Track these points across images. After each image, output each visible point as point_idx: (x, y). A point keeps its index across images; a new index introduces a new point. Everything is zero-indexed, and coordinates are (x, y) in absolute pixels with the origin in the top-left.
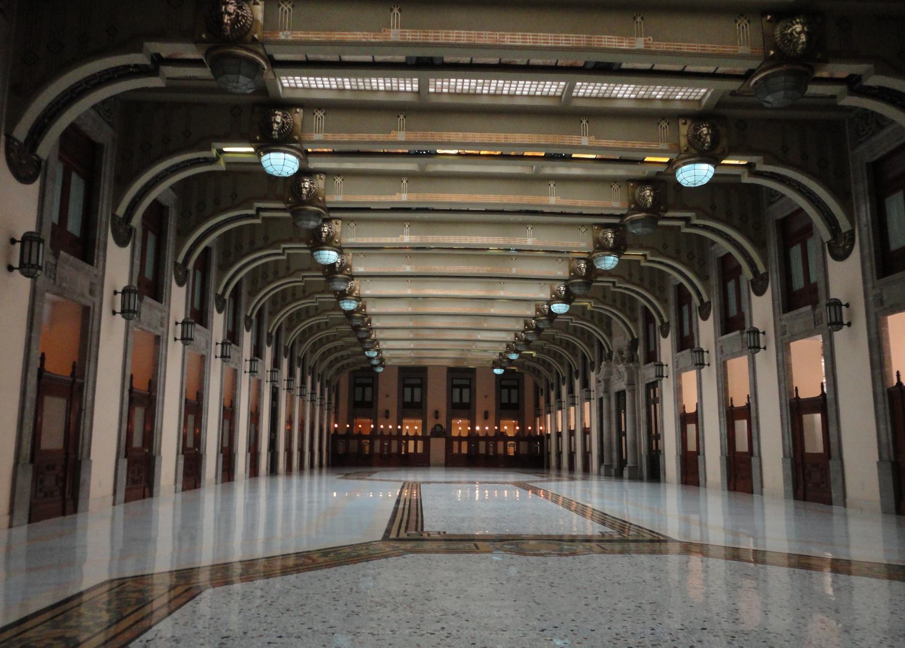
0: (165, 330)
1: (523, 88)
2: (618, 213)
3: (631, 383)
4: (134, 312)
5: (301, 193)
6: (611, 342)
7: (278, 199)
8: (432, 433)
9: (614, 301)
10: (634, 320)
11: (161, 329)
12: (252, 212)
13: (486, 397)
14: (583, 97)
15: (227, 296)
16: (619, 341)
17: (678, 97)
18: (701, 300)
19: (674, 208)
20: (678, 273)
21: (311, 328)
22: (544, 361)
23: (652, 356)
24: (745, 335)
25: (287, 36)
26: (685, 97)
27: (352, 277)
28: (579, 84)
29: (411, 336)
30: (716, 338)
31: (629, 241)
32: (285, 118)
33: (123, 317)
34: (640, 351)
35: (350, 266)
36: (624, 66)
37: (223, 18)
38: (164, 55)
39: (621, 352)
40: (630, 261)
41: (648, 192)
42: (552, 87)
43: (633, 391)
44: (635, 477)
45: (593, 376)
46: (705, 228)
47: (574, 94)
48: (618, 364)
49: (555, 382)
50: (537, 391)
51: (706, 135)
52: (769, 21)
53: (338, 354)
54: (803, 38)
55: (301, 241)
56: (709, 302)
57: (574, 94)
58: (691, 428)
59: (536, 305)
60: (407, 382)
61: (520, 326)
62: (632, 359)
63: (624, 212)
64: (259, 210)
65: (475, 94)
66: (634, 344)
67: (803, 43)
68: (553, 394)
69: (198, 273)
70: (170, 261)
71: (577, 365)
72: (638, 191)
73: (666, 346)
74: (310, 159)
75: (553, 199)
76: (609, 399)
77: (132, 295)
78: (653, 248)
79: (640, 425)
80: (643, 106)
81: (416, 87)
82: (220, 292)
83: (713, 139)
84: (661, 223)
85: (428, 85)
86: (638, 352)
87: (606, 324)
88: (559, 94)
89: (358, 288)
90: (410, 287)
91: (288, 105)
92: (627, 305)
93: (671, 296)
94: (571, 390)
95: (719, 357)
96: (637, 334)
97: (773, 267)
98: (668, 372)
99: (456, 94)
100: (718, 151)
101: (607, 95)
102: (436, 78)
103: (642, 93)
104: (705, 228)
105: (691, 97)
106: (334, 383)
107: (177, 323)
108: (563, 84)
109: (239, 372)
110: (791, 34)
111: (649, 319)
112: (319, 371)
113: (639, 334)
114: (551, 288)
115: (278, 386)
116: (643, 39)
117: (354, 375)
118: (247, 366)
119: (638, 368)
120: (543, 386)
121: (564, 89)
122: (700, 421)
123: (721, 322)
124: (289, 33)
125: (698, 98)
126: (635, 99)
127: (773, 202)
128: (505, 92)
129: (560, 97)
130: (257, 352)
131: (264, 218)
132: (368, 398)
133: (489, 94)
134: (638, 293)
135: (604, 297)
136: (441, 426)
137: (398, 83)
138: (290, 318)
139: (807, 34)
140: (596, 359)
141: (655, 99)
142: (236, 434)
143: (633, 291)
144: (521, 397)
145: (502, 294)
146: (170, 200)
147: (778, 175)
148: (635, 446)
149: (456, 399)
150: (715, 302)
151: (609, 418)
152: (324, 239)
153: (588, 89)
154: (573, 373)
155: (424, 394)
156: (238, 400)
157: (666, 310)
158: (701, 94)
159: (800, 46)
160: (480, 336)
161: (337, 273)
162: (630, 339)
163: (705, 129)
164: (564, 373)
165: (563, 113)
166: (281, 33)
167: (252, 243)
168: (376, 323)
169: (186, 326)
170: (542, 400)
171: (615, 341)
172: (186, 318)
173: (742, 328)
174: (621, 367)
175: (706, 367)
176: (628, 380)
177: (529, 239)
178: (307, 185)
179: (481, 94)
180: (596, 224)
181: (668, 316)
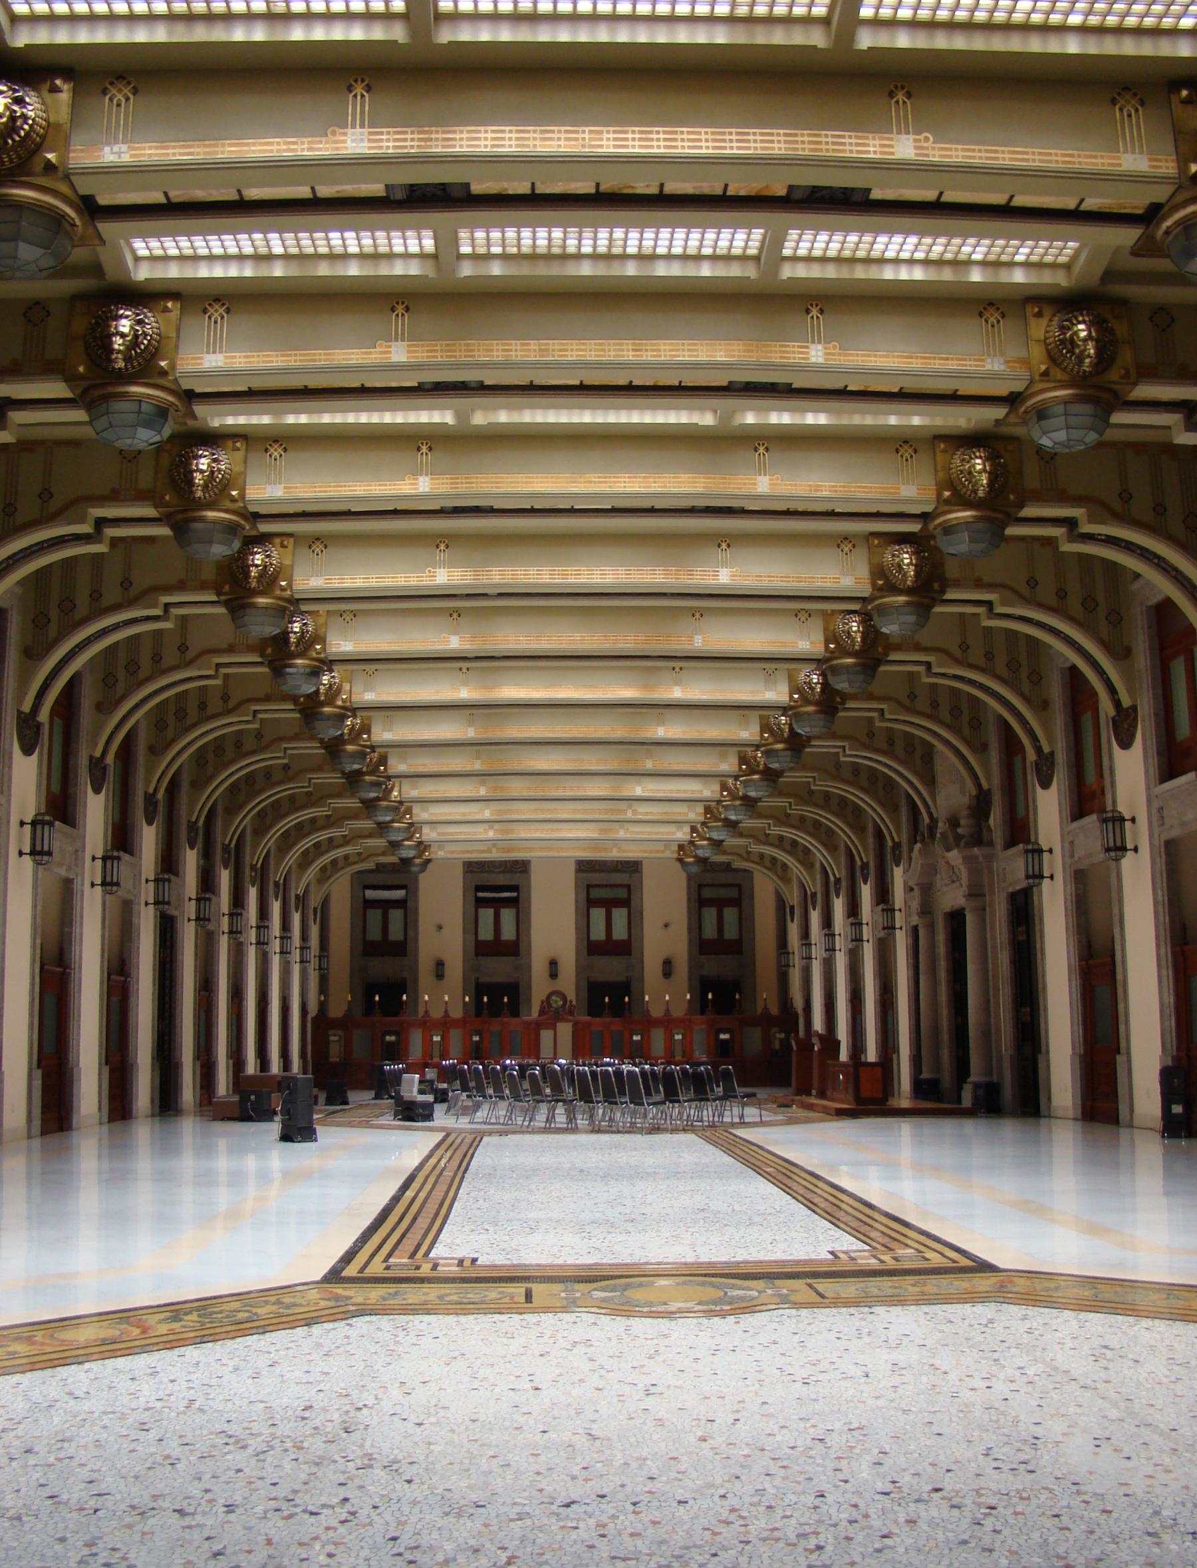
2: (917, 510)
3: (976, 893)
5: (190, 482)
7: (142, 496)
8: (542, 1012)
9: (935, 705)
10: (981, 749)
12: (86, 528)
13: (666, 926)
14: (809, 259)
15: (44, 716)
16: (951, 797)
17: (1020, 258)
18: (1117, 704)
19: (1039, 497)
20: (1067, 643)
21: (250, 779)
23: (1020, 831)
25: (120, 153)
27: (328, 664)
28: (793, 234)
29: (483, 792)
30: (1148, 789)
31: (952, 570)
32: (140, 322)
34: (996, 819)
35: (322, 640)
36: (876, 194)
39: (954, 822)
40: (962, 615)
42: (739, 239)
44: (989, 1105)
45: (898, 877)
46: (1111, 541)
47: (787, 252)
48: (948, 850)
49: (819, 888)
50: (783, 910)
51: (1085, 340)
53: (322, 836)
55: (203, 586)
56: (1134, 708)
57: (787, 252)
61: (728, 765)
62: (979, 838)
63: (929, 508)
64: (101, 523)
65: (564, 257)
68: (815, 917)
71: (865, 854)
73: (1048, 807)
74: (200, 409)
75: (763, 483)
76: (931, 927)
78: (1003, 586)
79: (997, 989)
80: (947, 275)
81: (429, 244)
82: (27, 707)
83: (1100, 350)
84: (1011, 531)
87: (922, 758)
88: (752, 252)
89: (346, 687)
91: (143, 297)
92: (964, 715)
93: (1056, 691)
94: (853, 909)
95: (1156, 831)
96: (988, 778)
98: (1051, 866)
99: (520, 257)
100: (1114, 375)
101: (861, 254)
102: (472, 227)
103: (937, 249)
104: (1111, 541)
105: (1049, 259)
106: (314, 901)
108: (757, 234)
109: (77, 886)
111: (1011, 746)
113: (993, 780)
114: (791, 679)
116: (911, 137)
117: (363, 882)
118: (92, 871)
119: (990, 858)
120: (794, 898)
121: (763, 242)
122: (1119, 977)
123: (1159, 753)
124: (124, 148)
125: (1062, 259)
128: (632, 250)
129: (757, 259)
130: (122, 839)
131: (115, 542)
134: (982, 687)
135: (912, 696)
136: (564, 998)
137: (389, 239)
138: (200, 758)
141: (969, 263)
142: (72, 1024)
144: (746, 922)
145: (677, 693)
148: (987, 1034)
149: (598, 933)
150: (1146, 708)
153: (815, 246)
155: (522, 923)
156: (75, 949)
157: (1047, 725)
161: (294, 656)
162: (974, 792)
163: (1081, 327)
164: (838, 870)
165: (765, 300)
166: (107, 149)
167: (95, 595)
168: (397, 765)
170: (793, 929)
171: (941, 799)
174: (955, 857)
176: (969, 887)
178: (204, 464)
179: (578, 257)
181: (1051, 739)
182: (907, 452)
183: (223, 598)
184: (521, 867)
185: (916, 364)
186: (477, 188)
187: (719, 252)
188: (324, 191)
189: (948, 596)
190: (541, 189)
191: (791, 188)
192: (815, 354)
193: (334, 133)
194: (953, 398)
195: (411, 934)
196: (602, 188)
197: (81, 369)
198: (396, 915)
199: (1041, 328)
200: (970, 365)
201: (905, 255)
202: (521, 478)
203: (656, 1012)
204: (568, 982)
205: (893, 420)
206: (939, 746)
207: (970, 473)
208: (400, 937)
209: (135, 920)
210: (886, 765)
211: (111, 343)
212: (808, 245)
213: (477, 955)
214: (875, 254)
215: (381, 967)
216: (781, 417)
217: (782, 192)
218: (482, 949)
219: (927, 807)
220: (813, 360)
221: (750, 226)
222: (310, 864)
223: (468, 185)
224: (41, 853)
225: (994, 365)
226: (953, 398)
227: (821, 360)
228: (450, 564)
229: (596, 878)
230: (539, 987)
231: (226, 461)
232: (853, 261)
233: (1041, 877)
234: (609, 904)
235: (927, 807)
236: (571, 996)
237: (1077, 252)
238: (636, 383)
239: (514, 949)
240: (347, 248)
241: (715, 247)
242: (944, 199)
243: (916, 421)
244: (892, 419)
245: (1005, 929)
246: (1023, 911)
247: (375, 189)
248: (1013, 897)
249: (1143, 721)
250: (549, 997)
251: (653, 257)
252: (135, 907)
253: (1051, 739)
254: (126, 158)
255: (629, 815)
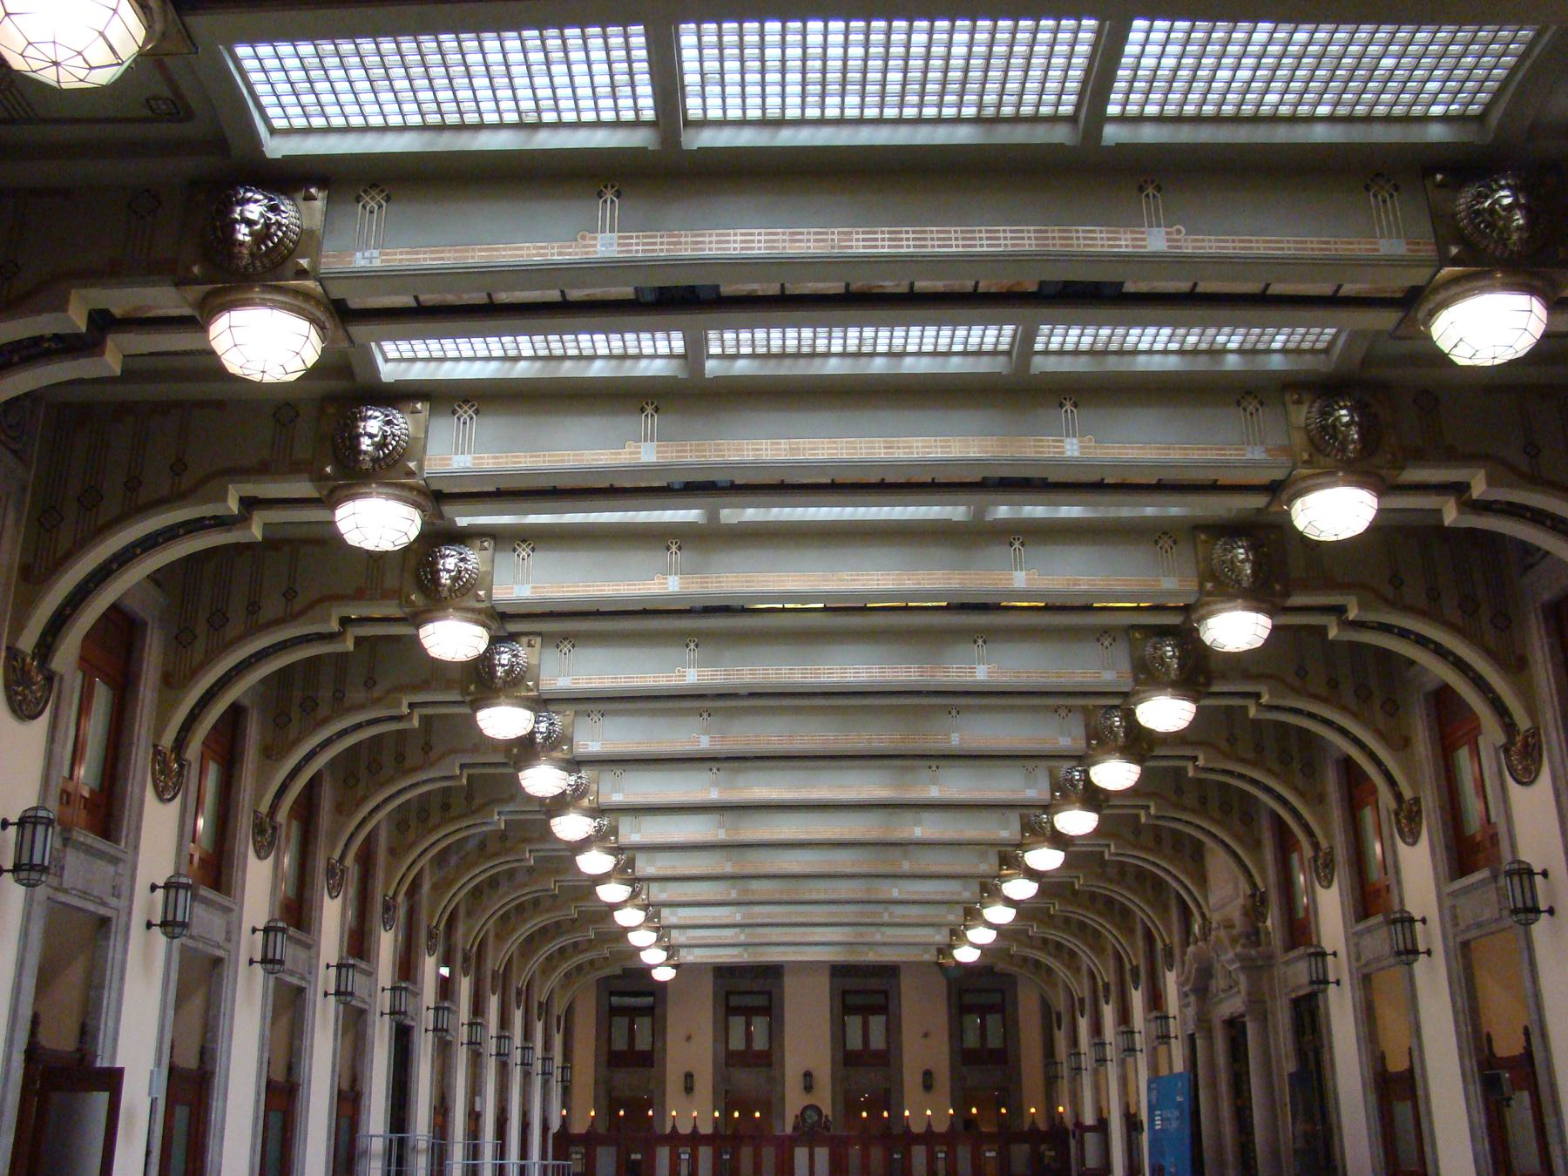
0: (123, 903)
1: (922, 345)
3: (1258, 1004)
4: (44, 869)
5: (436, 580)
6: (1206, 898)
8: (795, 1128)
10: (1255, 845)
11: (113, 902)
14: (1061, 353)
17: (1276, 345)
18: (1398, 797)
19: (1305, 586)
22: (1059, 946)
23: (1300, 931)
24: (1502, 881)
25: (371, 259)
26: (1291, 345)
28: (1045, 329)
29: (734, 895)
30: (1438, 887)
32: (389, 423)
33: (18, 881)
35: (571, 741)
36: (1129, 287)
37: (234, 231)
38: (117, 311)
41: (1241, 553)
43: (1263, 1019)
45: (1171, 982)
49: (1087, 994)
50: (1050, 1020)
51: (1347, 425)
52: (1441, 185)
53: (565, 940)
54: (1519, 219)
56: (1417, 800)
57: (1038, 347)
58: (1403, 1110)
59: (1022, 816)
60: (734, 1001)
63: (1191, 600)
65: (813, 355)
66: (1256, 906)
67: (1519, 228)
68: (1083, 1024)
69: (213, 770)
70: (143, 742)
71: (1136, 956)
72: (1218, 551)
73: (1330, 908)
74: (448, 510)
75: (1023, 577)
77: (40, 829)
78: (1271, 677)
80: (1202, 364)
81: (678, 345)
85: (707, 340)
86: (1269, 923)
87: (1194, 856)
88: (1003, 347)
89: (594, 787)
90: (715, 784)
95: (1450, 932)
96: (1264, 879)
97: (1549, 716)
99: (769, 356)
101: (1113, 347)
102: (722, 328)
103: (1192, 339)
105: (1306, 345)
106: (558, 1008)
107: (153, 888)
108: (1008, 330)
109: (309, 994)
110: (1491, 210)
112: (519, 981)
113: (1268, 880)
114: (1052, 774)
115: (408, 1022)
116: (1163, 230)
120: (1060, 1003)
121: (1014, 337)
122: (1420, 1093)
123: (1447, 847)
124: (376, 253)
125: (1320, 346)
126: (1181, 352)
127: (1531, 566)
128: (881, 348)
129: (1008, 353)
132: (643, 1043)
133: (844, 355)
136: (818, 1111)
139: (1527, 210)
140: (1176, 939)
141: (1224, 351)
143: (1241, 776)
145: (934, 793)
146: (148, 608)
147: (1527, 508)
151: (1213, 1084)
152: (499, 683)
153: (1066, 340)
154: (1128, 977)
155: (775, 1032)
158: (1327, 338)
159: (1515, 237)
160: (895, 891)
162: (1249, 892)
163: (1343, 412)
164: (1107, 975)
166: (359, 255)
169: (172, 893)
170: (1061, 1038)
171: (1213, 900)
172: (177, 874)
173: (1493, 860)
175: (1422, 957)
176: (1249, 994)
177: (980, 668)
178: (450, 563)
179: (828, 355)
180: (1133, 627)
182: (1166, 542)
183: (468, 698)
184: (773, 972)
185: (1175, 455)
186: (727, 290)
187: (970, 348)
188: (575, 294)
189: (1215, 689)
190: (792, 289)
191: (1042, 284)
192: (1069, 445)
193: (583, 238)
194: (1214, 488)
195: (659, 1045)
196: (853, 287)
197: (328, 469)
198: (643, 1025)
199: (1302, 414)
200: (1230, 455)
201: (1158, 347)
202: (772, 576)
203: (918, 1128)
204: (824, 1098)
205: (1150, 511)
206: (1209, 843)
207: (1232, 562)
208: (647, 1047)
209: (369, 1031)
210: (1154, 864)
211: (359, 444)
212: (1060, 339)
213: (727, 1065)
214: (1128, 346)
215: (625, 1079)
216: (1036, 511)
217: (1033, 288)
218: (730, 1060)
219: (1199, 906)
220: (1068, 454)
221: (1000, 323)
222: (554, 969)
223: (717, 287)
224: (273, 961)
225: (1256, 454)
226: (1214, 488)
227: (1076, 454)
228: (700, 664)
229: (853, 983)
230: (794, 1101)
231: (474, 558)
232: (1105, 353)
233: (1327, 982)
234: (866, 1011)
235: (1199, 906)
236: (827, 1110)
237: (1335, 337)
238: (888, 480)
239: (766, 1060)
240: (596, 351)
241: (966, 344)
242: (1199, 289)
243: (1174, 511)
244: (1149, 510)
245: (1289, 1036)
246: (1308, 1016)
247: (627, 292)
248: (1296, 1003)
249: (1428, 815)
250: (806, 1108)
251: (903, 354)
252: (370, 1019)
253: (1329, 836)
254: (377, 263)
255: (886, 918)
